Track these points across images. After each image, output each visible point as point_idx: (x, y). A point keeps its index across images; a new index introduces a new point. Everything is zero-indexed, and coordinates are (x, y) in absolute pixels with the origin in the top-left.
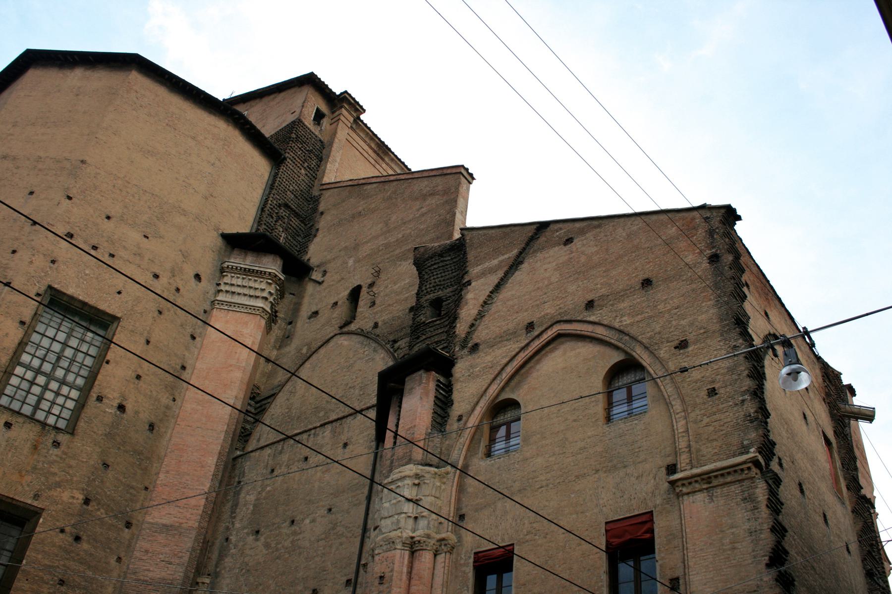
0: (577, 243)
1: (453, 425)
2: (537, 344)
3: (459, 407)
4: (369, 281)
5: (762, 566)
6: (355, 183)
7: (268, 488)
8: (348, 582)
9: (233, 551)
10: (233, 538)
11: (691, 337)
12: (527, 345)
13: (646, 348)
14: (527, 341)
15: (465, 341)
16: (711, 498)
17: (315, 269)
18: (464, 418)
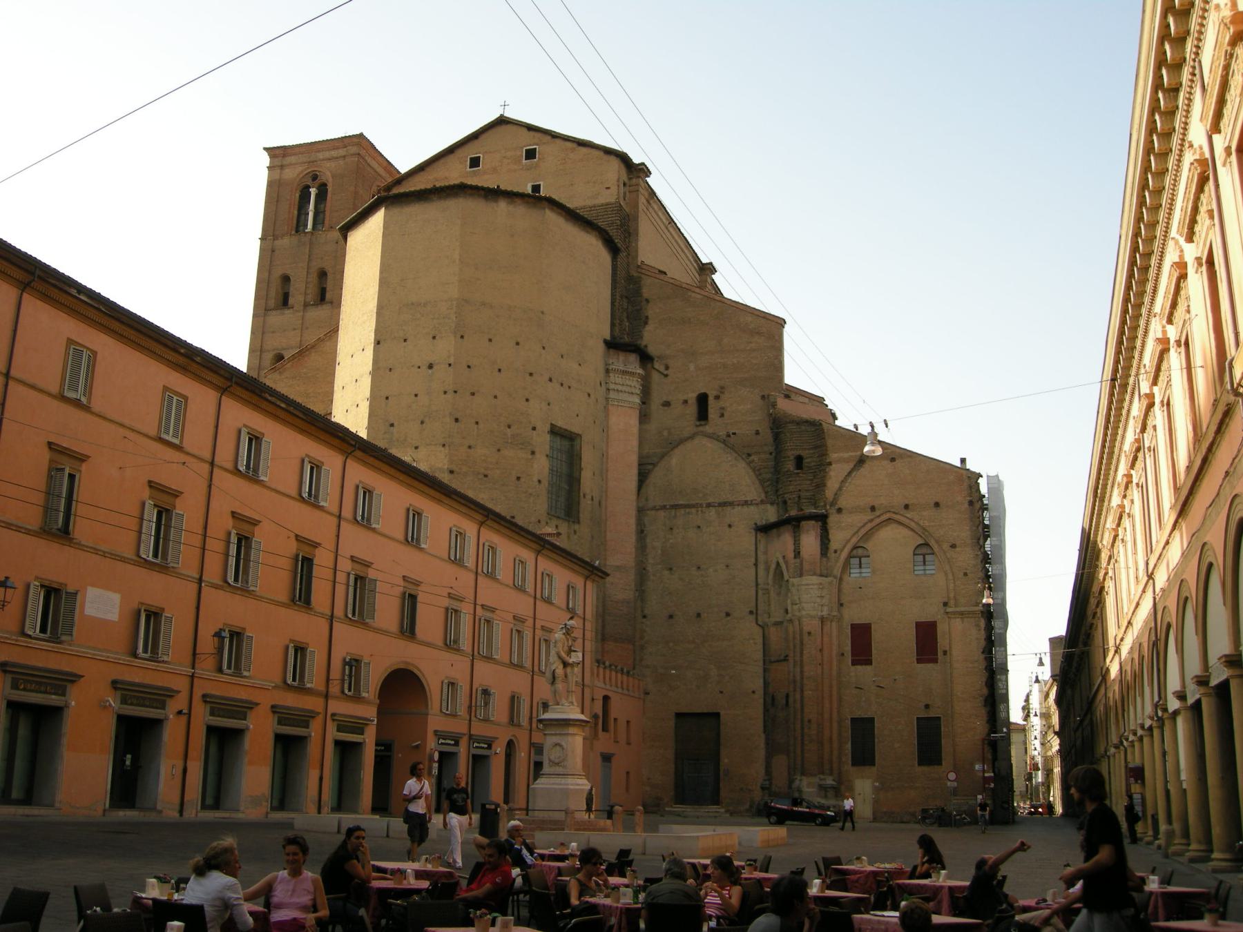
0: (898, 463)
1: (831, 554)
2: (878, 521)
3: (834, 545)
4: (715, 393)
5: (980, 653)
6: (677, 283)
7: (671, 541)
8: (751, 612)
9: (652, 578)
10: (649, 568)
11: (958, 543)
12: (871, 521)
13: (937, 542)
14: (872, 517)
15: (832, 504)
16: (963, 622)
17: (656, 359)
18: (839, 552)
